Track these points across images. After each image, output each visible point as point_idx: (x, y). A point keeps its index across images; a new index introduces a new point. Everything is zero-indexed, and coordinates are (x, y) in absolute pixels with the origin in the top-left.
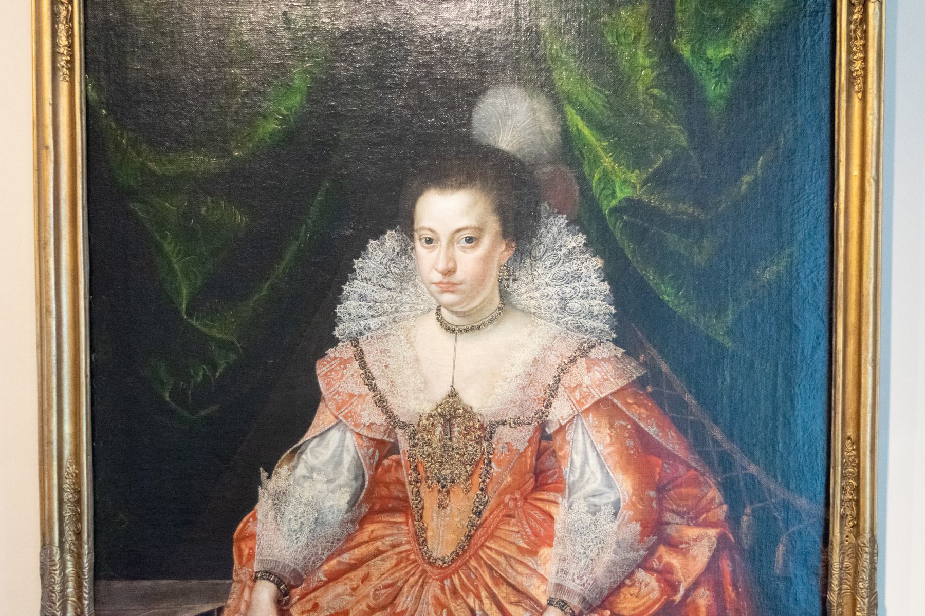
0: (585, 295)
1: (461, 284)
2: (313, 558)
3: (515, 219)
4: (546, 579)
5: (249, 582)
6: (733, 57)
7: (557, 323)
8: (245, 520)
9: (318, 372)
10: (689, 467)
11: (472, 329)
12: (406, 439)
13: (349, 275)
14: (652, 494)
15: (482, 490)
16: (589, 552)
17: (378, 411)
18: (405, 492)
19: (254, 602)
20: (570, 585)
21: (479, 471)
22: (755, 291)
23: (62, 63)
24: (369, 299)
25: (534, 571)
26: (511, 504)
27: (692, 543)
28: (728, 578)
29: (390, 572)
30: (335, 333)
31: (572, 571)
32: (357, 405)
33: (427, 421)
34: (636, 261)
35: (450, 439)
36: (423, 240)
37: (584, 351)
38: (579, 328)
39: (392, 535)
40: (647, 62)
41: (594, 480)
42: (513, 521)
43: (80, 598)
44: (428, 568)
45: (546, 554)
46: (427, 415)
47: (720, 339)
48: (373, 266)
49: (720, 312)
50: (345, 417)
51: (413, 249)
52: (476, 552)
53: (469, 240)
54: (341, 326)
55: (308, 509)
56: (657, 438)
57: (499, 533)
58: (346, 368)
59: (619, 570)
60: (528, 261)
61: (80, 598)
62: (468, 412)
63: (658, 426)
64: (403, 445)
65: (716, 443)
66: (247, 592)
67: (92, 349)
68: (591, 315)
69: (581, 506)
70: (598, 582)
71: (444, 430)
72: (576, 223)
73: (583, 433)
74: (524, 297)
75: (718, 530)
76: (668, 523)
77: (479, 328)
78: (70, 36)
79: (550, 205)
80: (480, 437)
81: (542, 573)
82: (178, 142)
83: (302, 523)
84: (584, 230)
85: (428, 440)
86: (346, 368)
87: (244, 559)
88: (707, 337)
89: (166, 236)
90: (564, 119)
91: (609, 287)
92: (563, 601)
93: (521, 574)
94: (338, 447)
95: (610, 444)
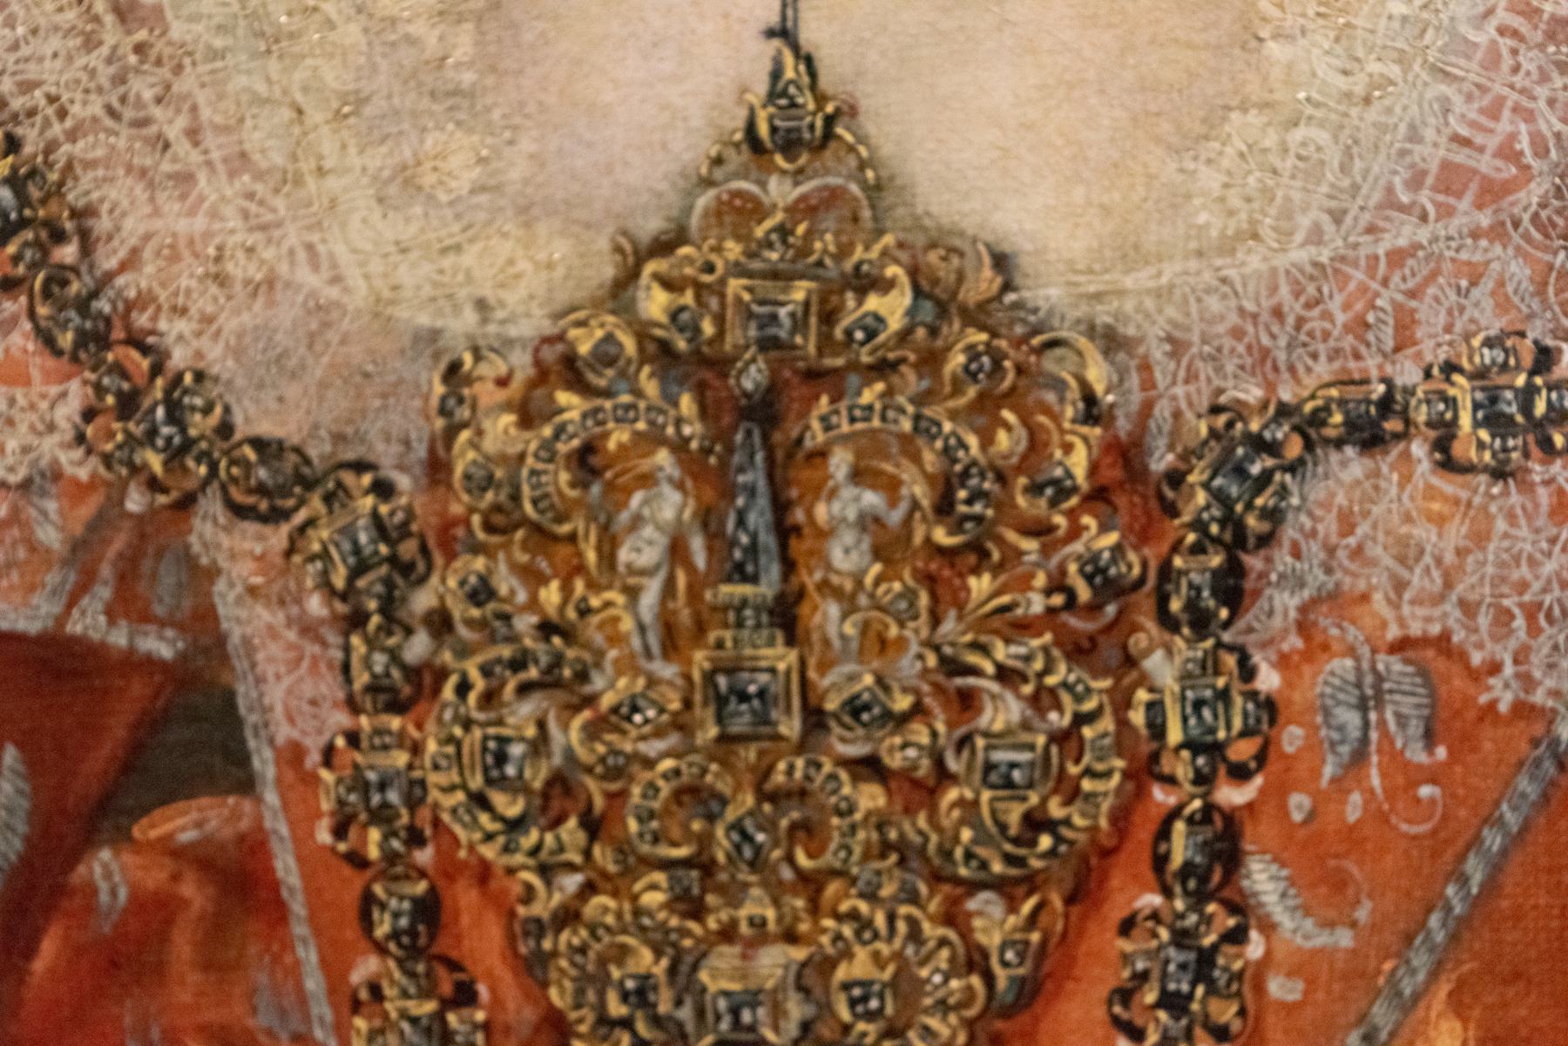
12: (309, 629)
33: (527, 420)
46: (522, 363)
62: (974, 316)
64: (275, 695)
71: (708, 520)
80: (1107, 585)
85: (547, 629)
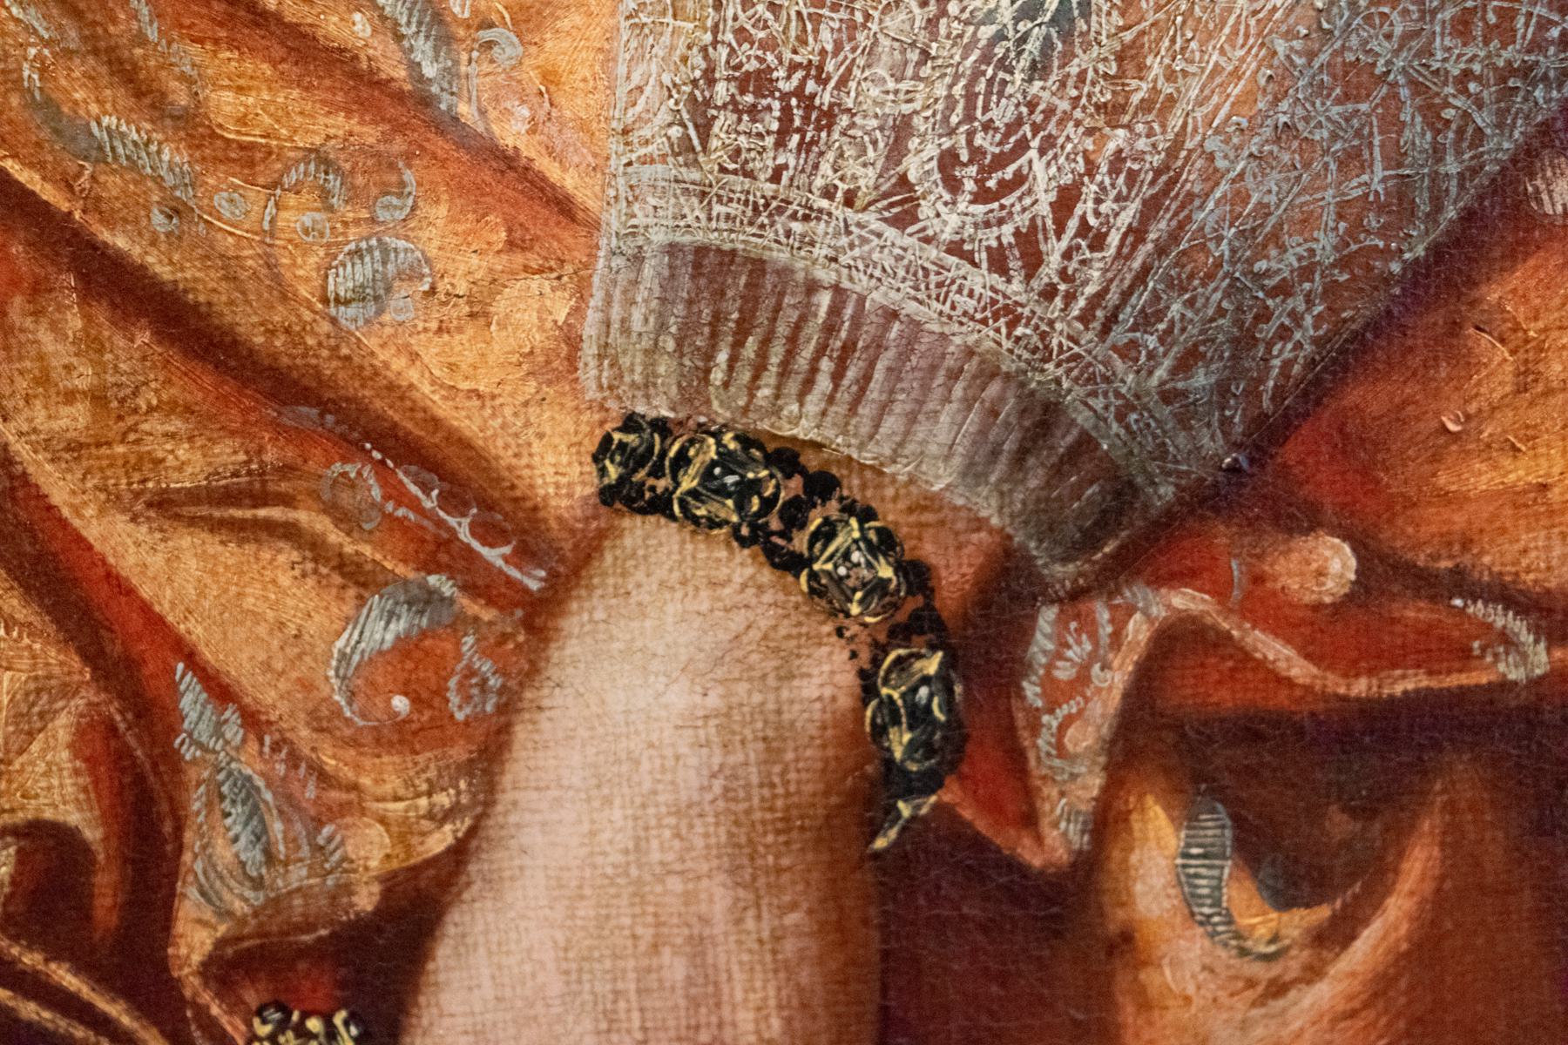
4: (563, 206)
59: (1449, 54)
70: (1205, 215)
81: (512, 132)
92: (786, 458)
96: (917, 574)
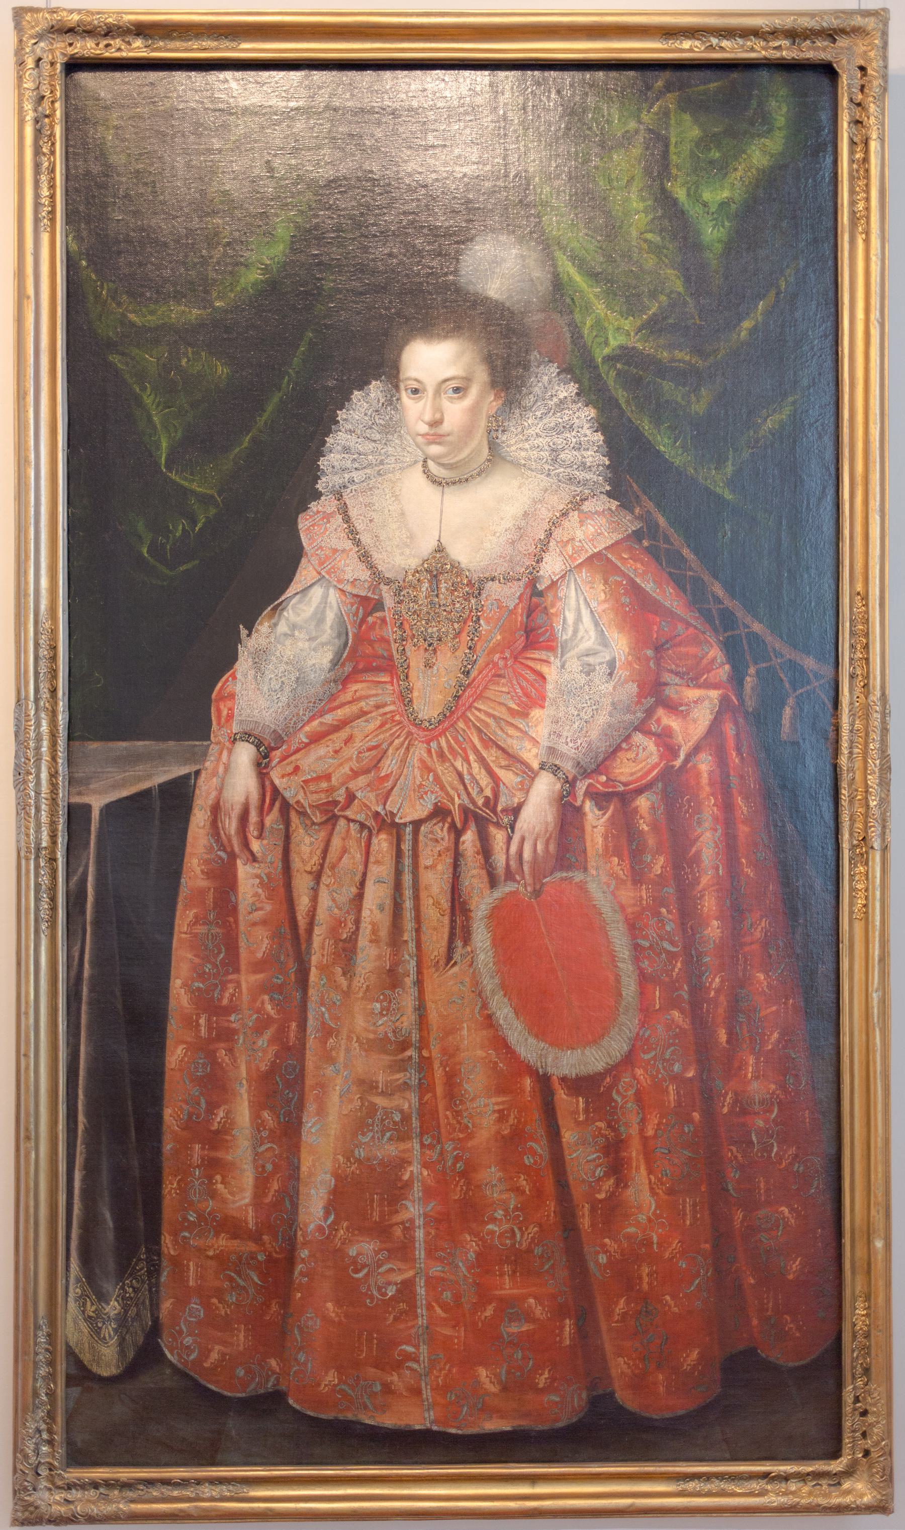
0: (577, 446)
1: (448, 435)
2: (294, 719)
3: (504, 369)
5: (227, 744)
6: (730, 200)
7: (548, 475)
8: (224, 679)
9: (300, 526)
10: (688, 625)
11: (460, 481)
13: (333, 427)
14: (650, 653)
15: (470, 648)
16: (582, 714)
17: (362, 566)
18: (389, 650)
19: (232, 765)
20: (563, 748)
21: (467, 629)
22: (757, 441)
23: (43, 214)
24: (353, 451)
25: (525, 733)
26: (501, 663)
27: (692, 705)
28: (731, 743)
29: (374, 734)
30: (318, 486)
31: (565, 734)
32: (340, 561)
34: (630, 411)
35: (437, 596)
36: (409, 391)
37: (576, 504)
38: (571, 480)
39: (376, 695)
40: (641, 206)
41: (588, 639)
42: (503, 681)
43: (54, 758)
44: (414, 730)
45: (538, 715)
47: (718, 490)
48: (357, 417)
49: (720, 463)
50: (328, 573)
51: (398, 400)
52: (464, 714)
53: (457, 390)
54: (324, 479)
55: (290, 668)
56: (654, 595)
57: (488, 694)
58: (329, 522)
59: (615, 733)
60: (517, 411)
61: (54, 758)
63: (655, 581)
65: (717, 600)
66: (225, 754)
67: (70, 502)
68: (583, 466)
69: (574, 665)
72: (567, 371)
73: (576, 589)
74: (513, 448)
75: (720, 692)
76: (666, 684)
77: (467, 480)
78: (52, 187)
79: (540, 354)
80: (468, 594)
81: (534, 736)
82: (158, 292)
83: (283, 683)
84: (577, 380)
86: (329, 522)
87: (223, 720)
88: (707, 489)
89: (146, 388)
90: (554, 266)
91: (602, 438)
92: (556, 766)
93: (511, 737)
94: (320, 603)
95: (605, 601)
96: (567, 777)
